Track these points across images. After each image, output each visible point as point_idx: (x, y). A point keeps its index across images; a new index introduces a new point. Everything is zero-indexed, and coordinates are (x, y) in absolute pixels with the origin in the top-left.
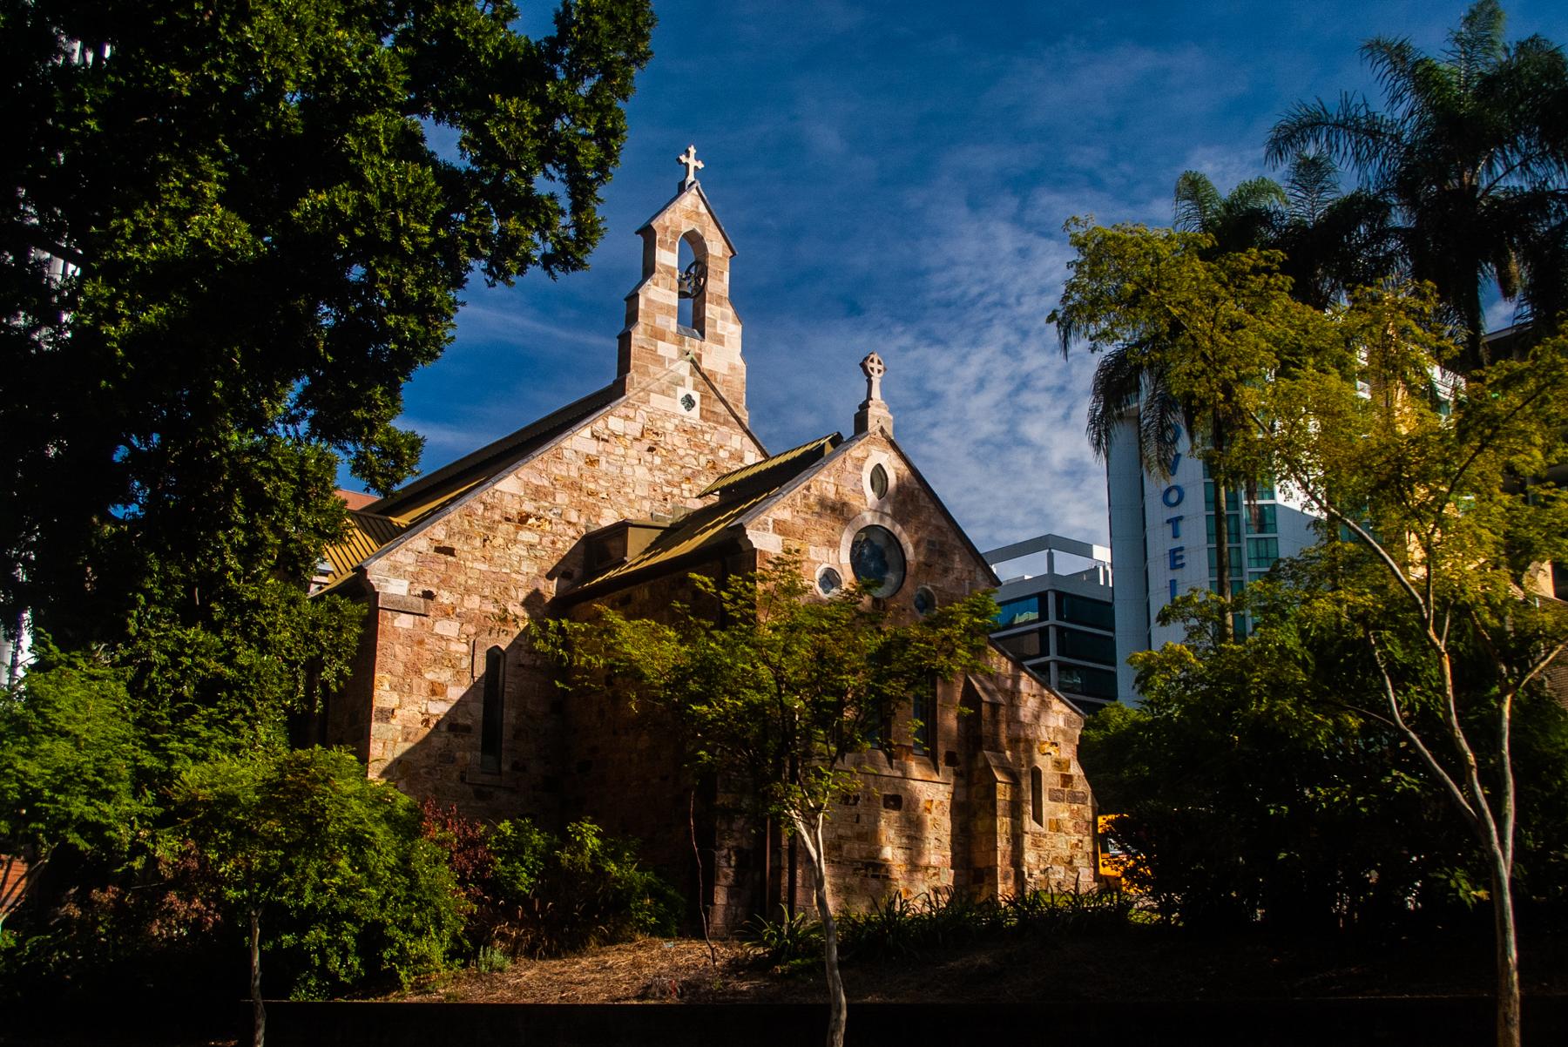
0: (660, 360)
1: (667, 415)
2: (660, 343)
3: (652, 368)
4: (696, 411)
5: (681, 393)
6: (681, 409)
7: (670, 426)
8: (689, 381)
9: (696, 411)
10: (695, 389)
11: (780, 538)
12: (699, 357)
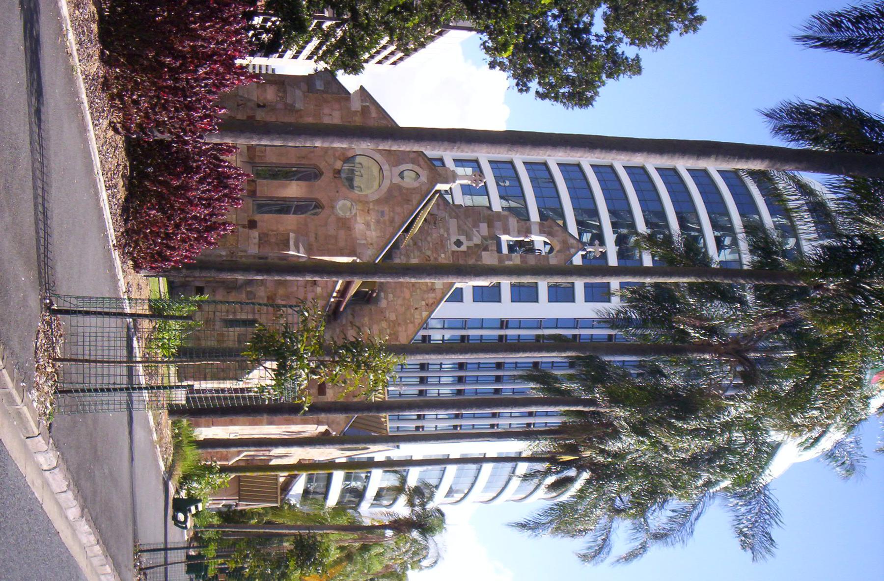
0: (476, 225)
1: (447, 230)
2: (486, 225)
3: (470, 219)
4: (455, 248)
5: (462, 238)
6: (454, 239)
7: (442, 231)
8: (471, 244)
9: (455, 248)
10: (468, 247)
11: (359, 109)
12: (486, 249)
